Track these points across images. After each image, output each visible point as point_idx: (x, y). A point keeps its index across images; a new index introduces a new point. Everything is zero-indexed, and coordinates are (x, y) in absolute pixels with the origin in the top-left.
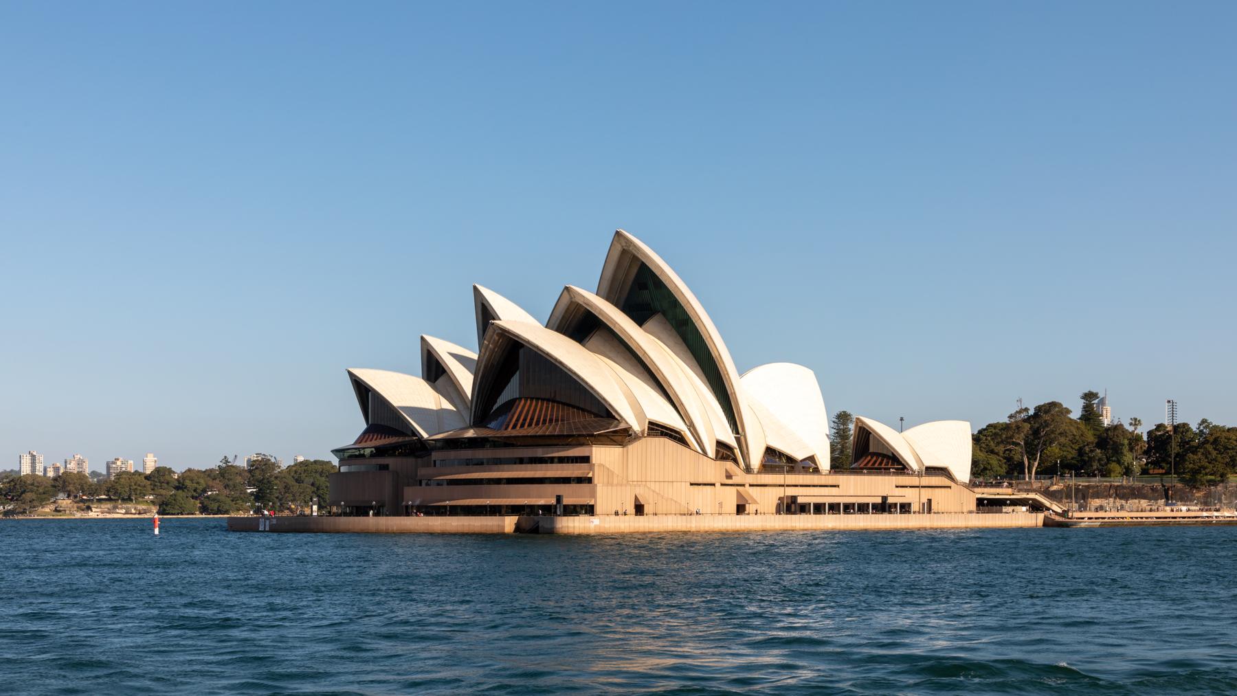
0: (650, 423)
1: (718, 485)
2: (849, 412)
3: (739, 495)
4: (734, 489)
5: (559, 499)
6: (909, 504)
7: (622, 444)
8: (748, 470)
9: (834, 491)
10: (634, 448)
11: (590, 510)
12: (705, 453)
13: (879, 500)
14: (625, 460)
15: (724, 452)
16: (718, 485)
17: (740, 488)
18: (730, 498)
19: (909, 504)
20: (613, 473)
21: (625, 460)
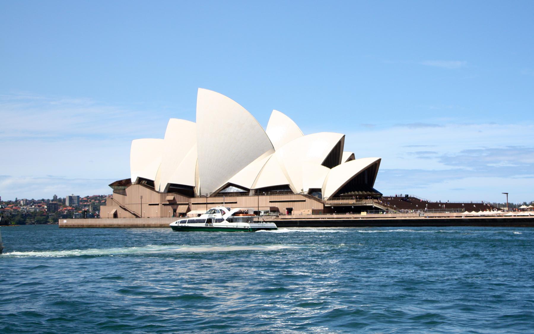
10: (128, 190)
15: (172, 188)
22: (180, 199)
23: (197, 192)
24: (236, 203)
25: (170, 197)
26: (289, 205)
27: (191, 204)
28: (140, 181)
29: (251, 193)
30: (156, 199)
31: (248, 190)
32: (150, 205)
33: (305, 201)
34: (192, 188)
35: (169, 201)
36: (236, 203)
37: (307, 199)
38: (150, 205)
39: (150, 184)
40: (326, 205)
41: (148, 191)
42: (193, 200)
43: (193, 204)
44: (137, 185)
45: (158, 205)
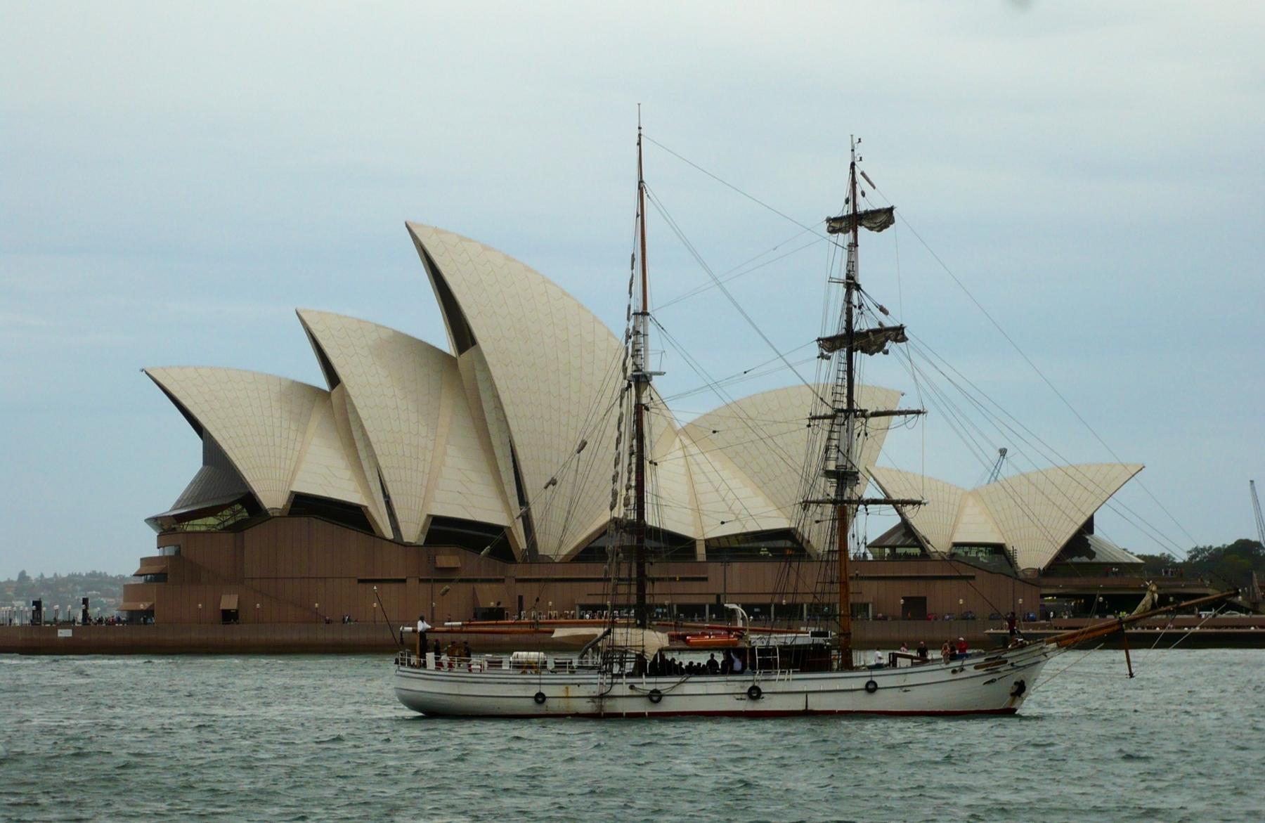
1: (413, 583)
4: (465, 588)
9: (696, 587)
12: (398, 541)
15: (445, 531)
16: (413, 583)
17: (478, 586)
23: (522, 543)
24: (705, 579)
25: (447, 559)
26: (915, 590)
28: (303, 504)
29: (701, 550)
32: (360, 581)
33: (973, 578)
36: (705, 579)
38: (360, 581)
39: (349, 517)
41: (354, 538)
42: (515, 570)
43: (518, 581)
44: (304, 520)
45: (404, 581)
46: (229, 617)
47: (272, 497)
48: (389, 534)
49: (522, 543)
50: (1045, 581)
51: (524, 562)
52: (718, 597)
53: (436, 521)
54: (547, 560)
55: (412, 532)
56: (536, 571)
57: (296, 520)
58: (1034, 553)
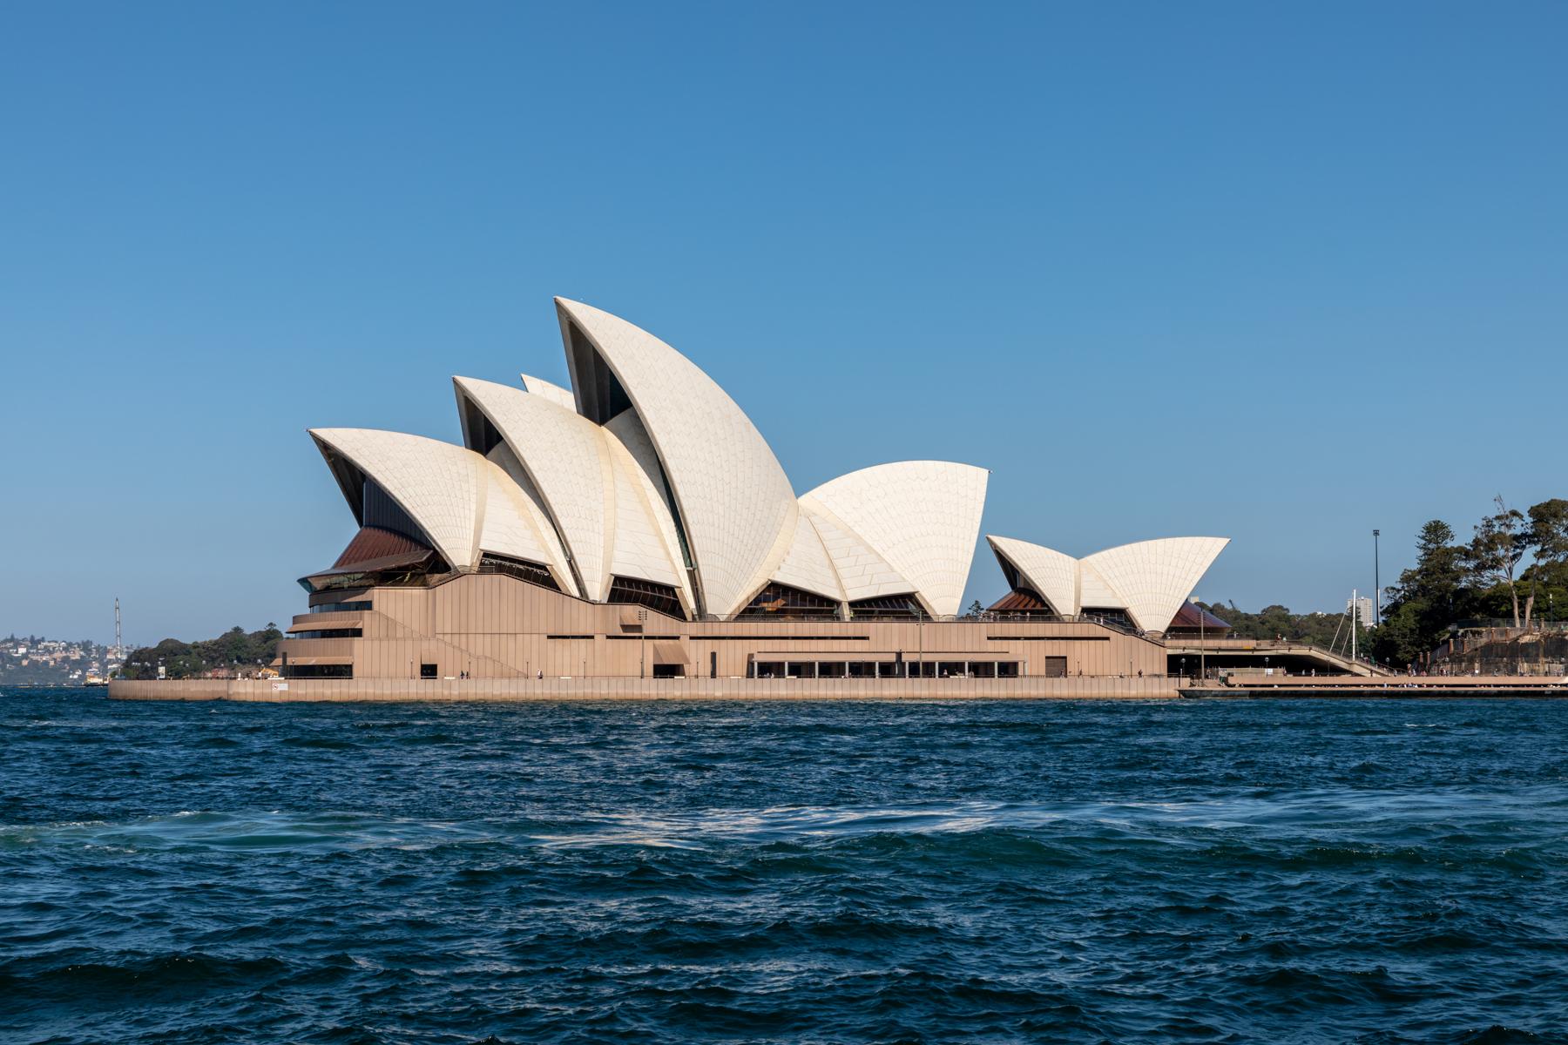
0: (486, 555)
1: (600, 639)
2: (1444, 520)
3: (656, 652)
5: (285, 656)
6: (1015, 664)
7: (425, 584)
8: (701, 614)
10: (447, 592)
11: (342, 671)
12: (583, 595)
13: (893, 658)
14: (431, 609)
15: (625, 590)
16: (600, 639)
18: (641, 655)
19: (1015, 664)
20: (395, 623)
21: (431, 609)
22: (656, 622)
23: (690, 603)
27: (685, 640)
29: (847, 612)
30: (584, 619)
31: (838, 603)
32: (550, 637)
34: (670, 589)
35: (625, 628)
37: (1112, 634)
38: (550, 637)
39: (536, 574)
40: (1170, 652)
44: (496, 577)
46: (429, 671)
47: (460, 553)
48: (577, 594)
49: (692, 604)
50: (1168, 642)
51: (694, 619)
52: (899, 655)
53: (619, 580)
54: (715, 619)
55: (598, 589)
56: (710, 630)
57: (487, 578)
58: (1154, 616)
